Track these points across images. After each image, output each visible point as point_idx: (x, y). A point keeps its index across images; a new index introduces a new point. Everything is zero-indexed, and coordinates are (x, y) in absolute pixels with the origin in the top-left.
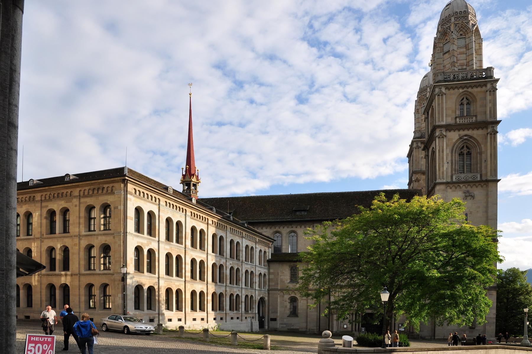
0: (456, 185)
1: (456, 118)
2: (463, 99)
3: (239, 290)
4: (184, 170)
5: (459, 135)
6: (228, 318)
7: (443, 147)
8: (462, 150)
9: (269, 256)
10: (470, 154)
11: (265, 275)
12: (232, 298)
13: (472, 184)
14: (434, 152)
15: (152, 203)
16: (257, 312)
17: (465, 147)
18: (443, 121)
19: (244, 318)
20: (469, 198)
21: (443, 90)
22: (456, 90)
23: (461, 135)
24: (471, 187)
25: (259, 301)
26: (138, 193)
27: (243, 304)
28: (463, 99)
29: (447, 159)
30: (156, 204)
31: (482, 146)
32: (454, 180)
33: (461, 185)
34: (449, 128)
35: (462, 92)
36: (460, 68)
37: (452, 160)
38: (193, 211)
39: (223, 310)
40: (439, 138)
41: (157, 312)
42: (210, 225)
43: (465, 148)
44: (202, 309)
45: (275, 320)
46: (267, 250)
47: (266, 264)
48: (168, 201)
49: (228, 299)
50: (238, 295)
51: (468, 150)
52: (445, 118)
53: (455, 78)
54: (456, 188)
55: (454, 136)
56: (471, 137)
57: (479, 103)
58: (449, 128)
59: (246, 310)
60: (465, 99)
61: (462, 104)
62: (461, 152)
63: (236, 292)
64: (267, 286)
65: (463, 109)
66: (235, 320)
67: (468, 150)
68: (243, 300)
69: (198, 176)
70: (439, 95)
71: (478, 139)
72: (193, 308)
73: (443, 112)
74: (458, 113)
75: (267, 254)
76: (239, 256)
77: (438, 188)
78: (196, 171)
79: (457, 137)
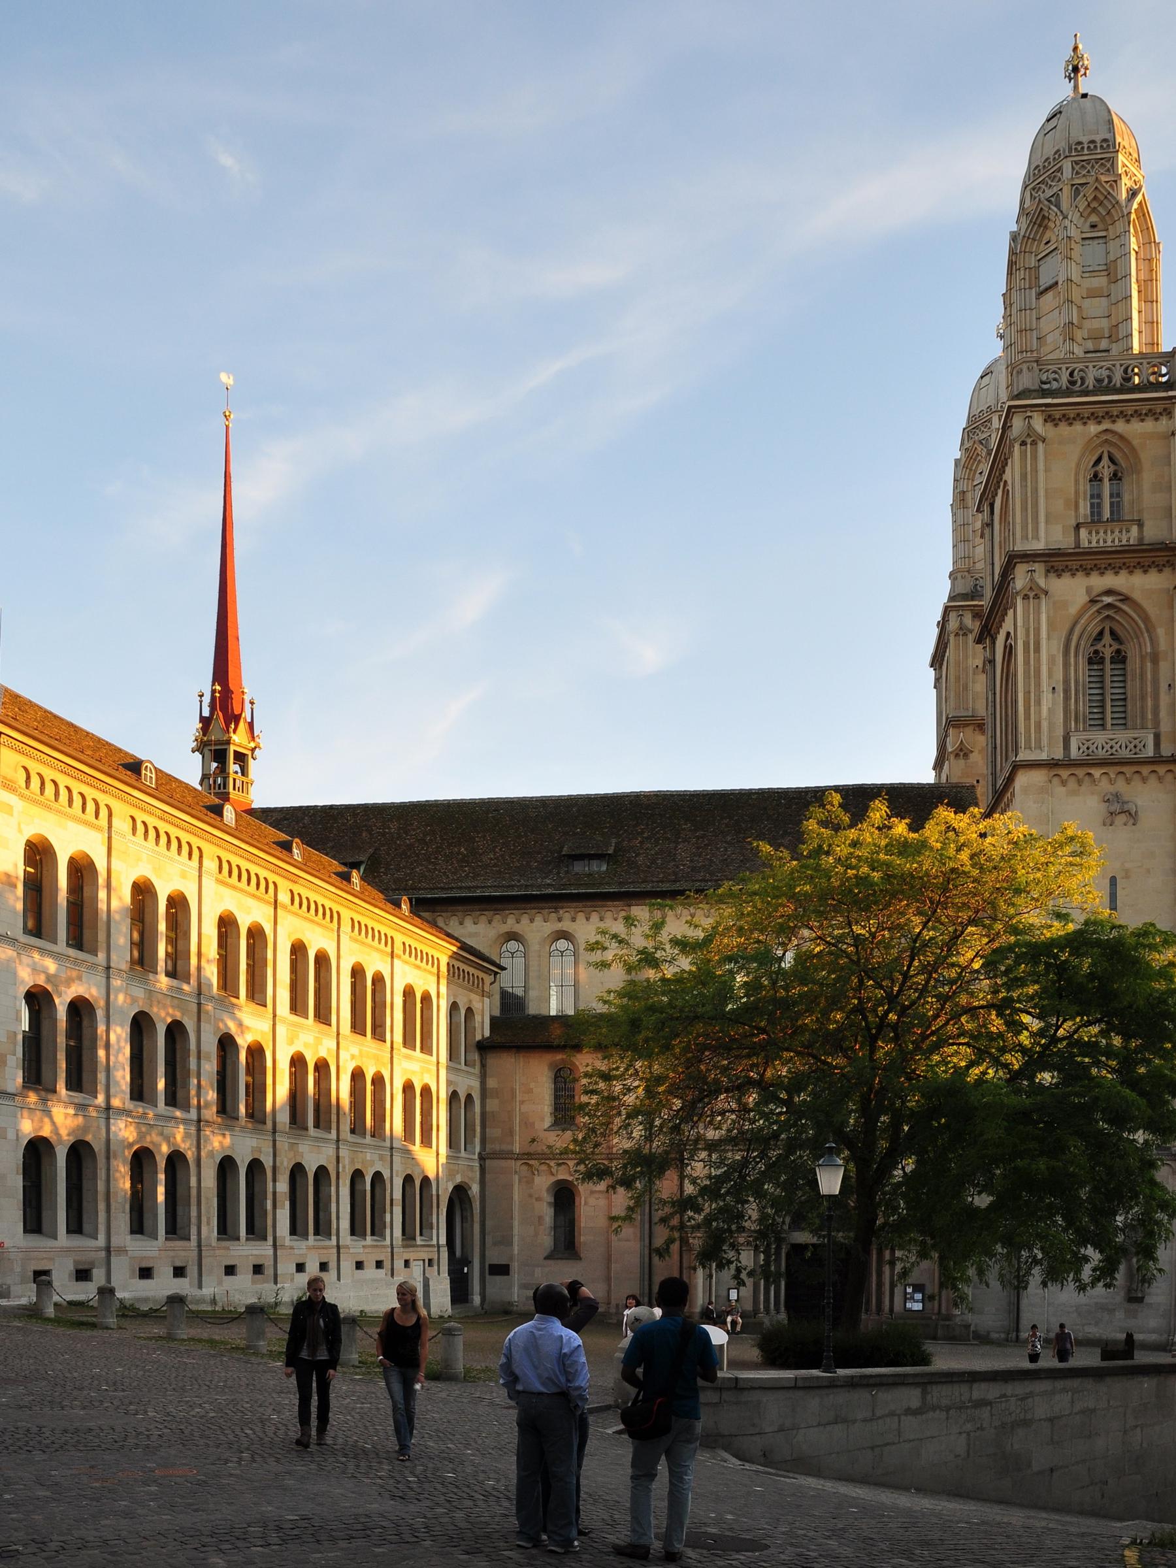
0: (1080, 772)
1: (1078, 527)
2: (1099, 460)
3: (381, 1158)
4: (207, 699)
5: (1089, 590)
6: (347, 1265)
7: (1037, 630)
8: (1099, 647)
9: (483, 1029)
10: (1124, 660)
11: (469, 1097)
12: (358, 1187)
13: (1129, 770)
14: (1009, 651)
15: (87, 823)
16: (443, 1240)
17: (1107, 632)
18: (1036, 537)
19: (399, 1264)
20: (1122, 819)
21: (1038, 423)
22: (1078, 427)
23: (1094, 593)
24: (1128, 781)
25: (451, 1200)
26: (35, 783)
27: (398, 1210)
28: (1099, 460)
29: (1050, 676)
30: (98, 829)
31: (1161, 632)
32: (1074, 753)
33: (1097, 773)
34: (1057, 561)
35: (1097, 436)
36: (1090, 345)
37: (1066, 681)
38: (225, 856)
39: (328, 1235)
40: (1026, 597)
41: (101, 1241)
42: (285, 907)
43: (1107, 639)
44: (256, 1230)
45: (502, 1270)
46: (476, 1006)
47: (476, 1056)
48: (140, 817)
49: (345, 1191)
50: (378, 1176)
51: (1116, 646)
52: (1042, 526)
53: (1073, 383)
54: (1080, 782)
55: (1073, 591)
56: (1126, 599)
57: (1148, 477)
58: (1057, 561)
59: (408, 1235)
60: (1105, 461)
61: (1096, 478)
62: (1096, 652)
63: (372, 1163)
64: (477, 1140)
65: (1099, 496)
66: (370, 1272)
67: (1116, 646)
68: (398, 1195)
69: (251, 725)
70: (1023, 443)
71: (1145, 604)
72: (225, 1229)
73: (1036, 504)
74: (1085, 509)
75: (478, 1018)
76: (383, 1025)
77: (1023, 780)
78: (247, 706)
79: (1082, 598)
